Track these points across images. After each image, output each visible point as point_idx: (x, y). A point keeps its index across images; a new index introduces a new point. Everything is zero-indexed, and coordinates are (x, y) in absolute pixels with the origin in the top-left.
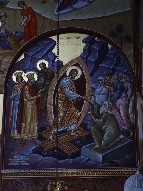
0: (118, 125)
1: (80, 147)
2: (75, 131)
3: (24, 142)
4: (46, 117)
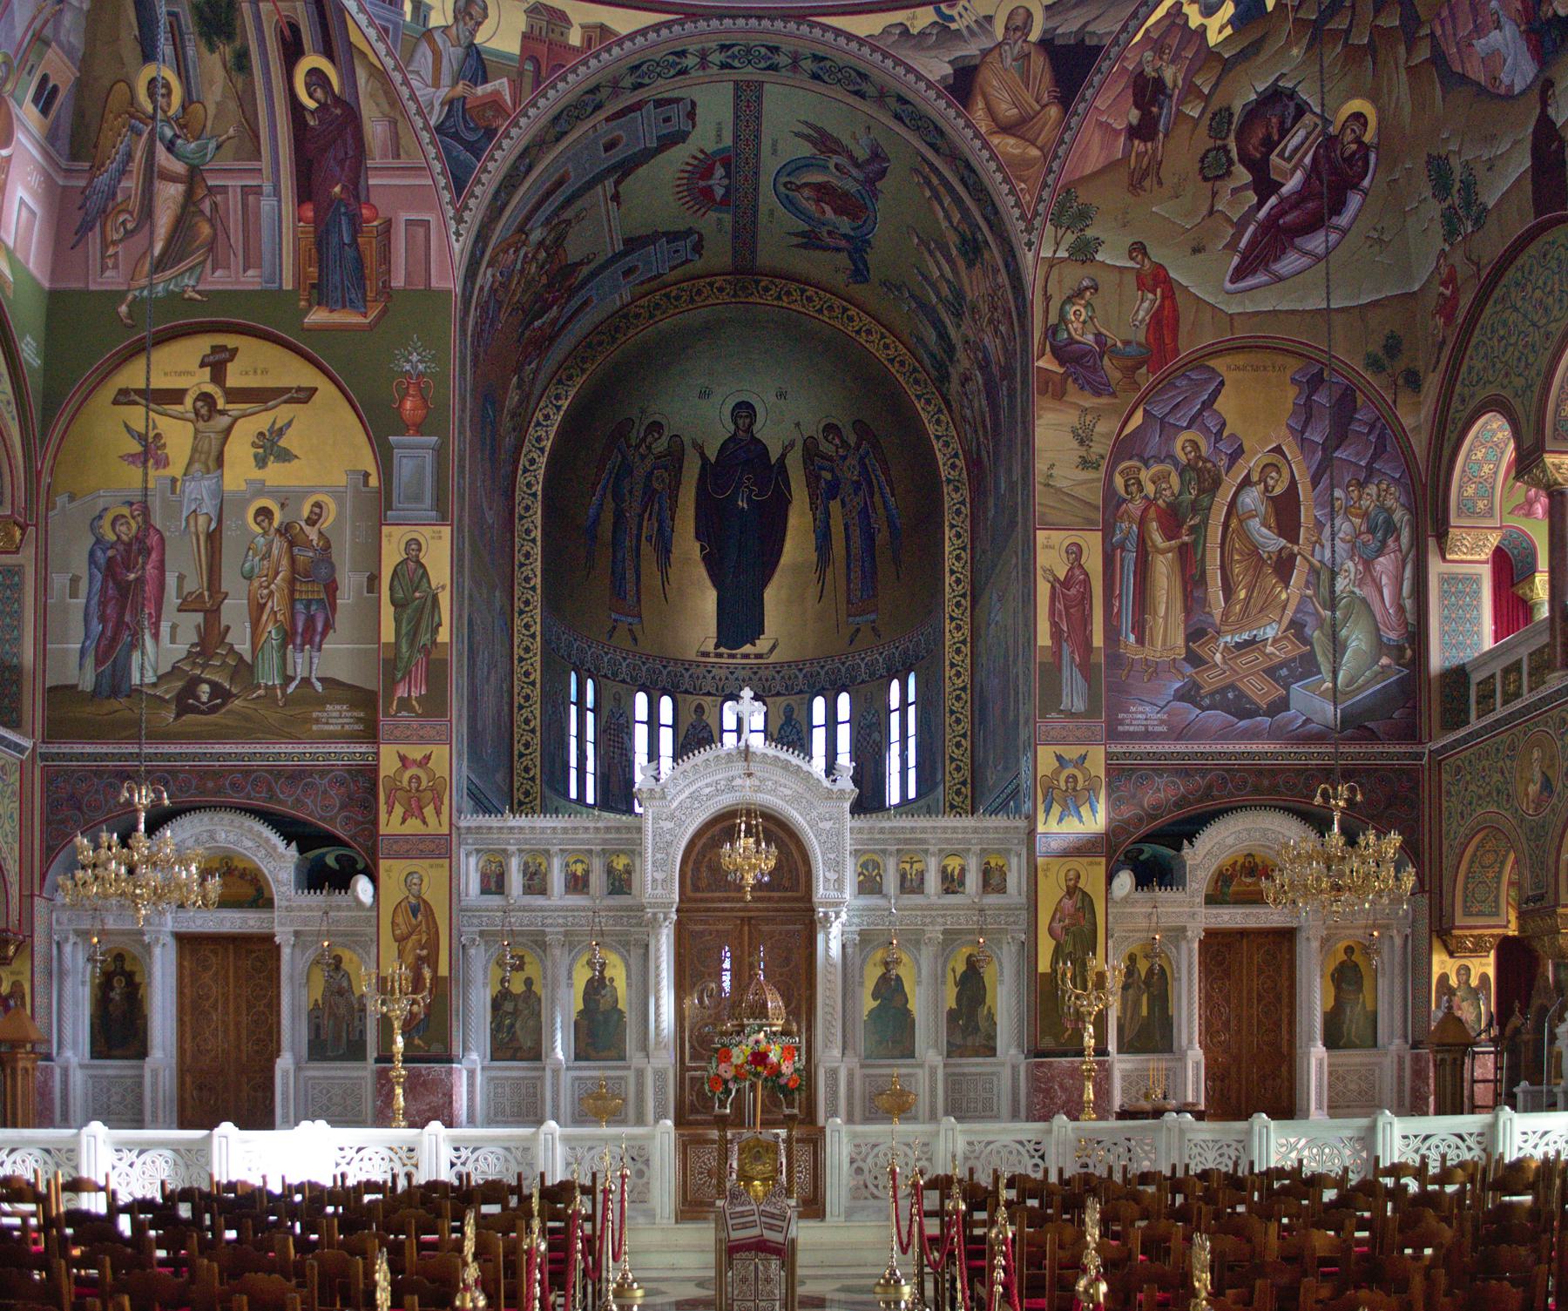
0: (1378, 629)
1: (1287, 687)
2: (1275, 641)
3: (1154, 670)
4: (1204, 601)
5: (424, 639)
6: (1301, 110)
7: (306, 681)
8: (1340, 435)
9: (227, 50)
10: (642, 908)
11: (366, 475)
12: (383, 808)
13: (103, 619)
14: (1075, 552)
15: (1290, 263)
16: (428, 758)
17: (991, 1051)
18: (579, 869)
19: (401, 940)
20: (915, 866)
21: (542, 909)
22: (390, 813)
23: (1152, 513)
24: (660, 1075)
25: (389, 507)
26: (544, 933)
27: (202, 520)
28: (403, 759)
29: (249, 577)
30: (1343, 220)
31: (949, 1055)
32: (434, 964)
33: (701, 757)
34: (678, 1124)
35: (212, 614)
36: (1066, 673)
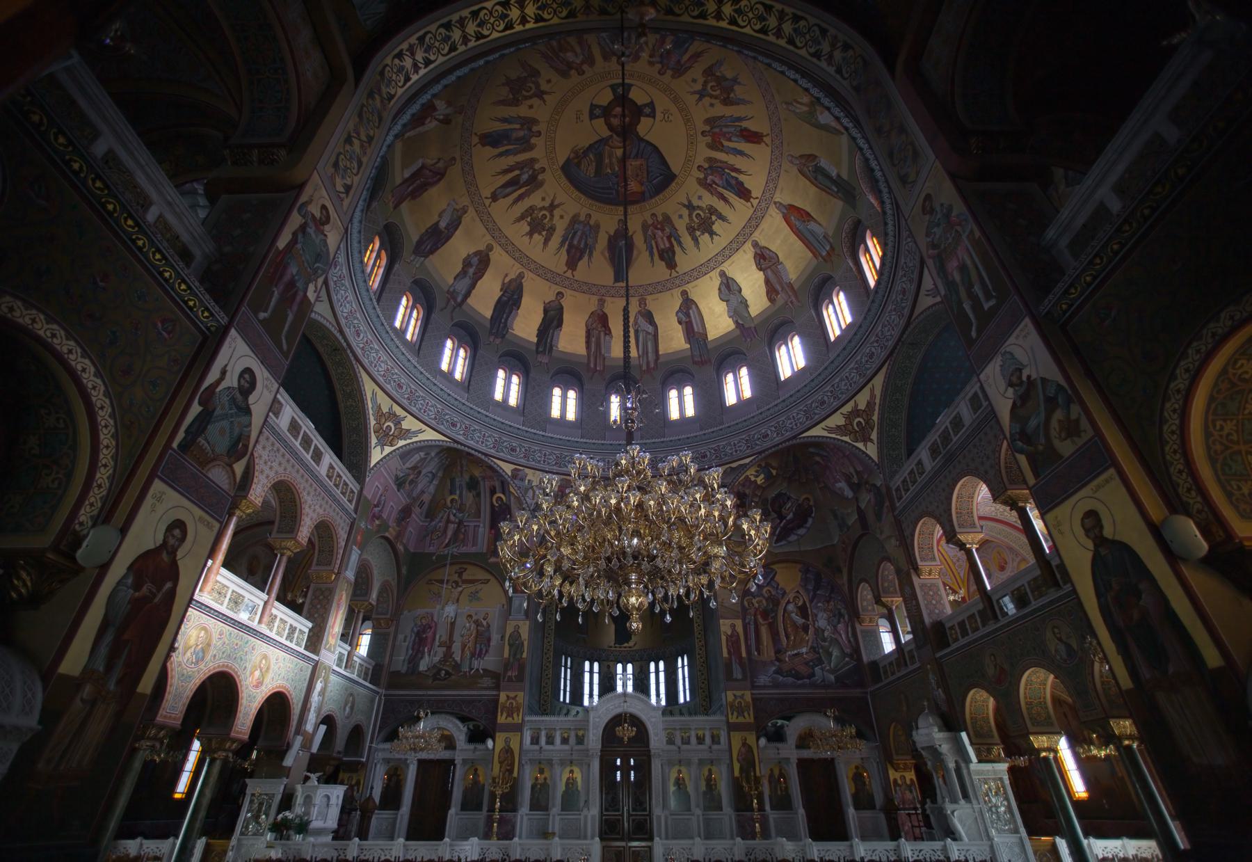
0: (842, 649)
1: (813, 668)
2: (806, 653)
5: (518, 656)
6: (789, 498)
7: (477, 670)
8: (817, 588)
9: (474, 493)
10: (588, 750)
11: (503, 605)
12: (499, 714)
13: (413, 649)
14: (733, 626)
15: (793, 538)
16: (516, 696)
17: (721, 809)
18: (566, 735)
19: (501, 763)
20: (687, 734)
21: (552, 751)
22: (501, 715)
23: (758, 613)
24: (593, 817)
25: (510, 615)
26: (552, 760)
27: (449, 619)
28: (508, 696)
29: (462, 636)
30: (808, 525)
31: (705, 810)
32: (511, 771)
33: (610, 695)
34: (602, 839)
35: (449, 648)
36: (734, 667)
